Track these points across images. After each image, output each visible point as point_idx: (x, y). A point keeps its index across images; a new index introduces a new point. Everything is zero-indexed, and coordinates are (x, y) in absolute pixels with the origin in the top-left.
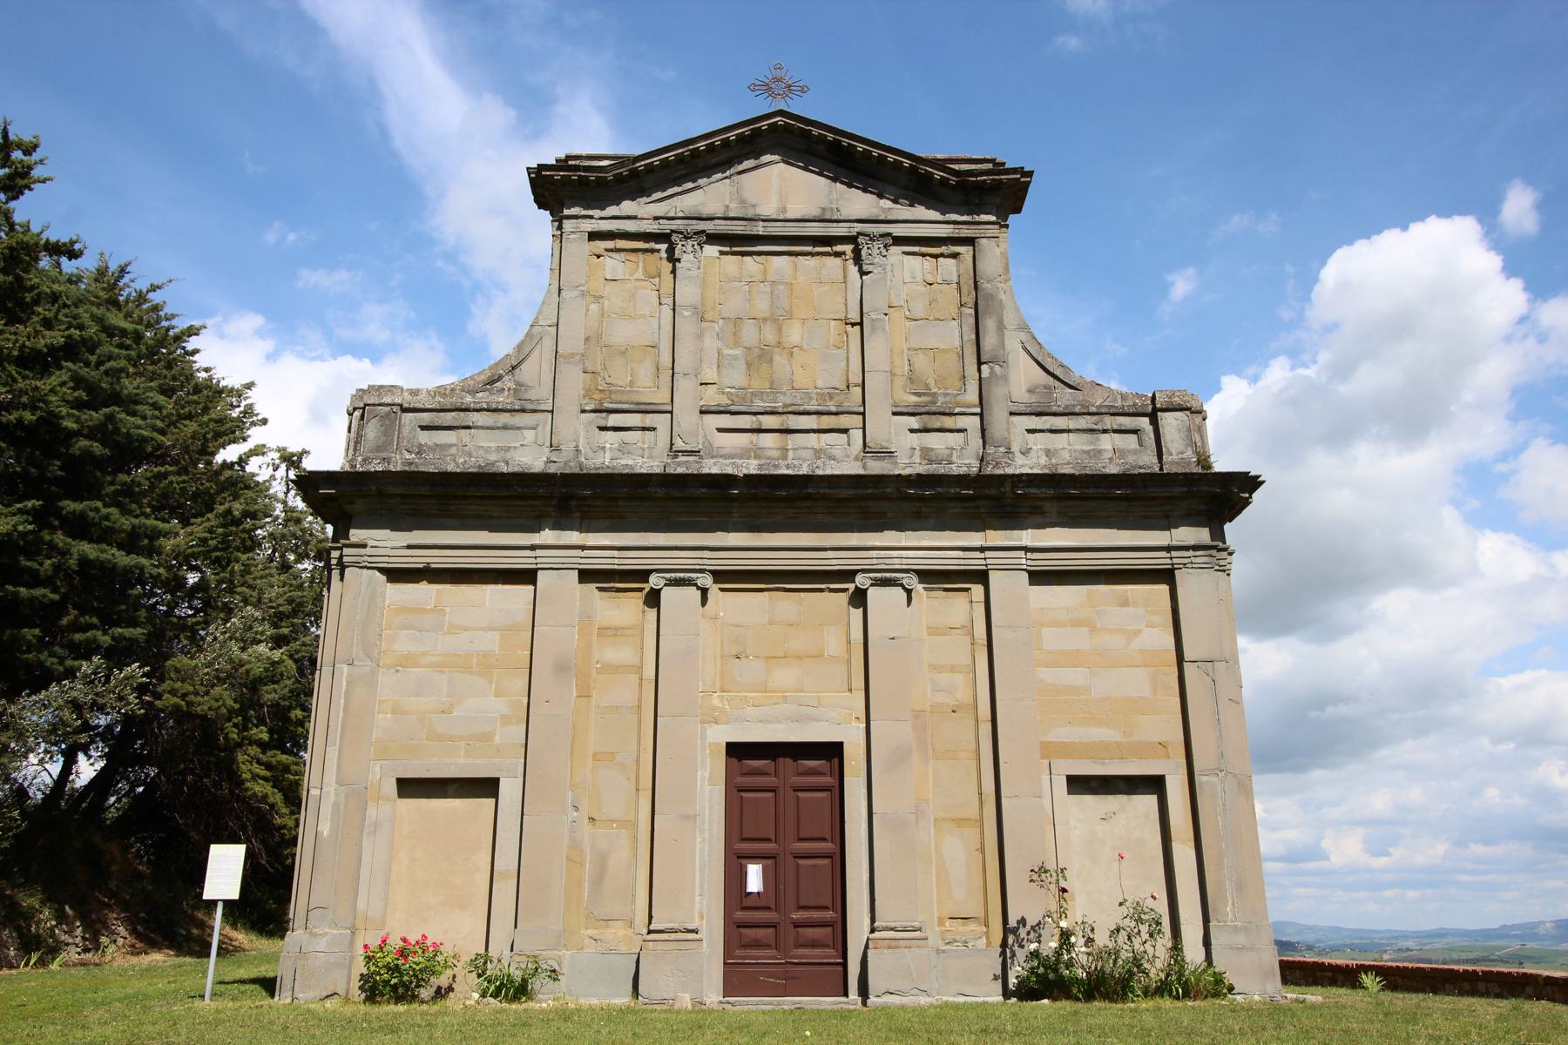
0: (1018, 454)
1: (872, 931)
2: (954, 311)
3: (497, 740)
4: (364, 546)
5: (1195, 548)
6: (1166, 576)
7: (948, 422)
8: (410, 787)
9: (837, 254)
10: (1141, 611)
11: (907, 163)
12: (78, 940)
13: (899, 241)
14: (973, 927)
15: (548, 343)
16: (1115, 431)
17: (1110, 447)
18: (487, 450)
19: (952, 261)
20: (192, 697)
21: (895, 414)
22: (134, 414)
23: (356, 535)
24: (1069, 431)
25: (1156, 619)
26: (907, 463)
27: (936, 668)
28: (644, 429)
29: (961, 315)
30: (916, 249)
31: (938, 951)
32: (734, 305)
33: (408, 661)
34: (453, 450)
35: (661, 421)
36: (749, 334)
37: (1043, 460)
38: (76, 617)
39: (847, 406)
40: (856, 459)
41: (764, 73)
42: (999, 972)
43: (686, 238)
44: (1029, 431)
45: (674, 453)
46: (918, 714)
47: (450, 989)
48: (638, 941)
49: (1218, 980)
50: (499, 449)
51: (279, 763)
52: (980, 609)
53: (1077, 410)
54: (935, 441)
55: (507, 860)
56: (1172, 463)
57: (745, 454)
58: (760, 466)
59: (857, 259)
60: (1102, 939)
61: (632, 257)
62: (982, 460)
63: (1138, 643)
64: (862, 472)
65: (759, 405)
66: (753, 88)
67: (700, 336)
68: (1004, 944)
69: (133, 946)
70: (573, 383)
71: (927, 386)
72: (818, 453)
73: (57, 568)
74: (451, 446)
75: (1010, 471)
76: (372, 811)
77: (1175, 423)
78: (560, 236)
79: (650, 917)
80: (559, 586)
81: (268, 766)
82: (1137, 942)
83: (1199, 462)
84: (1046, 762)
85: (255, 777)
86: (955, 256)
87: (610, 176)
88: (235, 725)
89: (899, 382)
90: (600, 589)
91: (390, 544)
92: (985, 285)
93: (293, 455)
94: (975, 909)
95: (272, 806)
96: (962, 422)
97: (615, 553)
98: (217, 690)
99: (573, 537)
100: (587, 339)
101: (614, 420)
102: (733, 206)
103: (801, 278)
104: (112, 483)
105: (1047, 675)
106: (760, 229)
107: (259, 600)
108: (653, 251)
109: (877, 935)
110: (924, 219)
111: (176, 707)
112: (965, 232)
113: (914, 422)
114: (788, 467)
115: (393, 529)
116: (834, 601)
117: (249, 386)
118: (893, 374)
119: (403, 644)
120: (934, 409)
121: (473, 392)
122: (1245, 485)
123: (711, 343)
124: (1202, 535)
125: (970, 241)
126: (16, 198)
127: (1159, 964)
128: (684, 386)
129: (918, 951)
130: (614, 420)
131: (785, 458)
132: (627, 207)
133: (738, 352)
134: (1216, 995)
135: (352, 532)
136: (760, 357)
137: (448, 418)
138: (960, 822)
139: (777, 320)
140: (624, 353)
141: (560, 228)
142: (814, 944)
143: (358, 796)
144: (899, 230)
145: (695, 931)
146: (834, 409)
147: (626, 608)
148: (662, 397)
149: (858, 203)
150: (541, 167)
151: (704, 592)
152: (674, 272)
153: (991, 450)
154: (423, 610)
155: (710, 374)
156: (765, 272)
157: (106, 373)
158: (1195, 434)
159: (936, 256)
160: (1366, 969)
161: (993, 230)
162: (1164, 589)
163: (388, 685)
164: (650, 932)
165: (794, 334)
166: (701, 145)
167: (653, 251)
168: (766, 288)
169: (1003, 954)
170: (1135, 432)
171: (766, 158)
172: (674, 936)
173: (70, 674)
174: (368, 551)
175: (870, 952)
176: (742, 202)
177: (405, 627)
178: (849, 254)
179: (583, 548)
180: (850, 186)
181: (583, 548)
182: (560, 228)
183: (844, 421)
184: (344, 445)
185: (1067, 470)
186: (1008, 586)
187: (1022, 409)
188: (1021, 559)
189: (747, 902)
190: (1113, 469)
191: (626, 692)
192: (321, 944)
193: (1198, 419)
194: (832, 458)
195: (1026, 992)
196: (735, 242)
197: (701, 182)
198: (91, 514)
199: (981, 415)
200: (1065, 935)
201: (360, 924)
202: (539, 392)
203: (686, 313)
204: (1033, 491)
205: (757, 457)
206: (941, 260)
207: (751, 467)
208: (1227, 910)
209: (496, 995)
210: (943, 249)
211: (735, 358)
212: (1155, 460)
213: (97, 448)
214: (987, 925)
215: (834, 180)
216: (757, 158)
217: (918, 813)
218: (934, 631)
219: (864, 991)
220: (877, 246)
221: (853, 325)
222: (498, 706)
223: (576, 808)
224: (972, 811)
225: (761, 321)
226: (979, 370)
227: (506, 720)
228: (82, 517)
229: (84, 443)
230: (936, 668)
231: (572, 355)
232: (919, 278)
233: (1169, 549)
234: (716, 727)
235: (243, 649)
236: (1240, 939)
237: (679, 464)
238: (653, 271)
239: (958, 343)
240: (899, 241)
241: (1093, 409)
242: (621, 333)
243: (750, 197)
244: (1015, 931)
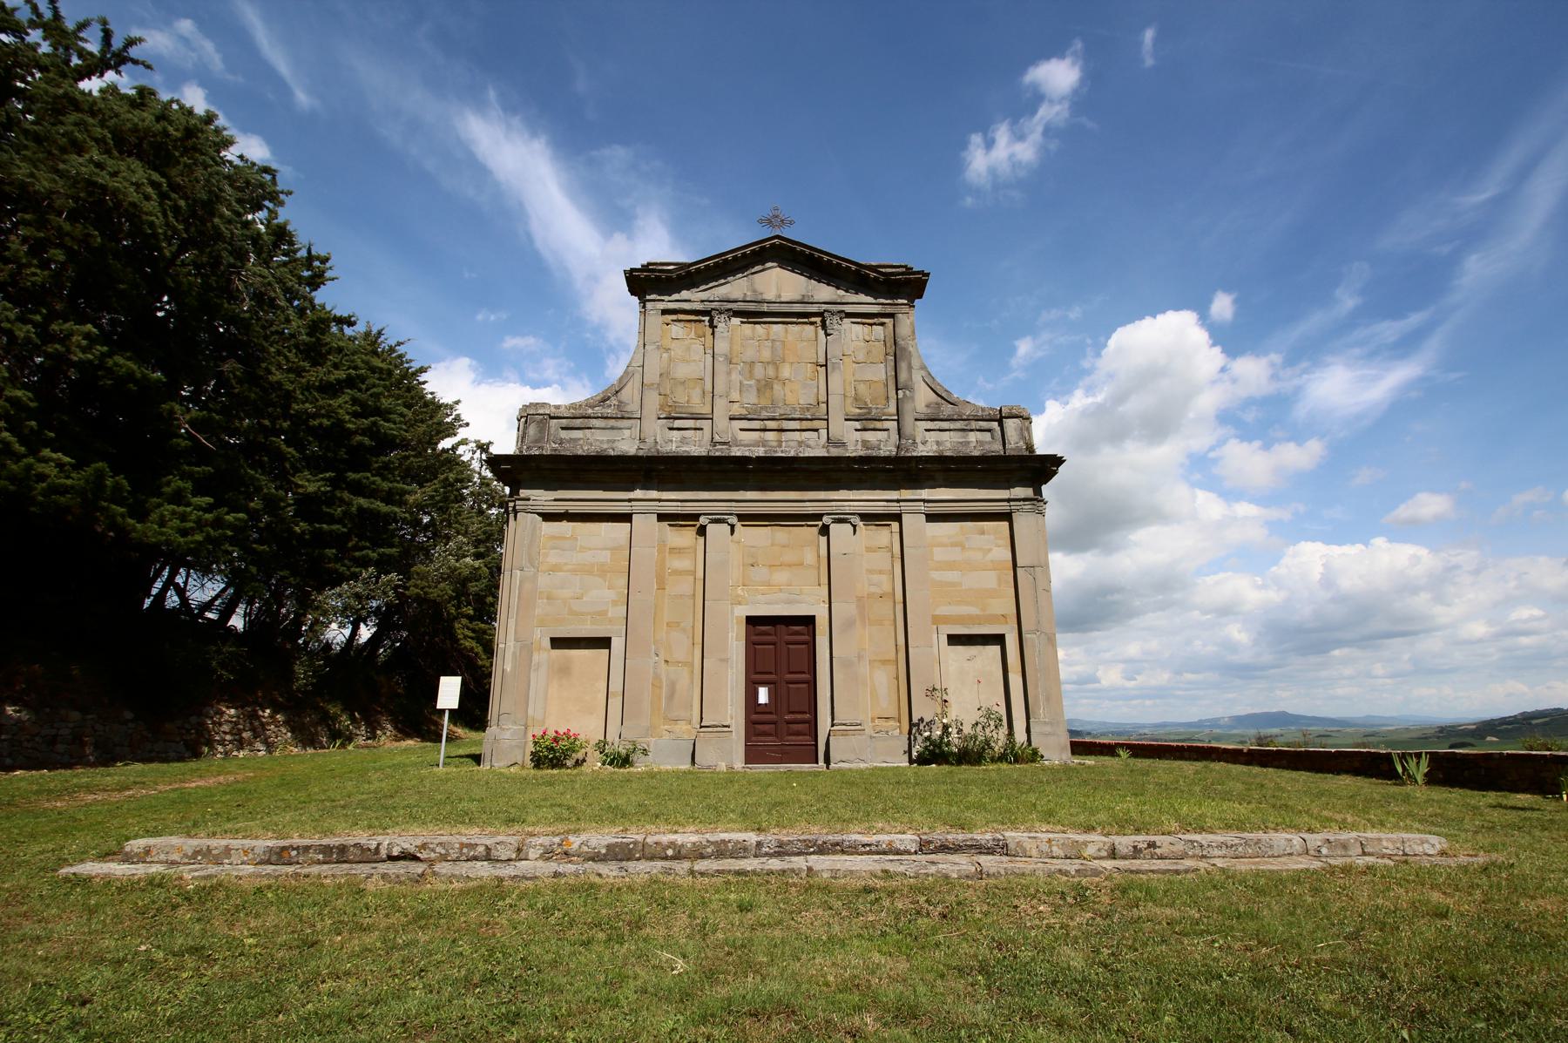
0: (920, 444)
1: (833, 726)
2: (882, 358)
3: (610, 615)
4: (529, 500)
5: (1025, 500)
6: (1007, 517)
7: (878, 425)
9: (812, 323)
10: (992, 537)
11: (853, 268)
12: (363, 733)
13: (849, 315)
14: (891, 723)
15: (638, 377)
16: (978, 430)
17: (974, 440)
18: (602, 442)
19: (881, 328)
20: (427, 589)
21: (846, 420)
22: (388, 421)
23: (523, 493)
24: (950, 430)
25: (1001, 542)
26: (853, 450)
27: (870, 572)
28: (696, 429)
29: (886, 360)
30: (859, 320)
31: (871, 737)
32: (750, 354)
33: (555, 568)
34: (581, 442)
35: (706, 424)
36: (759, 371)
37: (935, 447)
38: (357, 542)
39: (818, 415)
40: (823, 447)
41: (768, 213)
42: (907, 749)
43: (721, 313)
44: (926, 430)
45: (714, 443)
46: (860, 599)
47: (584, 760)
48: (694, 732)
49: (1035, 752)
50: (608, 441)
51: (480, 629)
52: (897, 537)
53: (955, 417)
54: (870, 436)
55: (616, 685)
56: (1012, 449)
57: (757, 444)
58: (766, 452)
59: (824, 326)
60: (967, 730)
61: (688, 325)
62: (898, 448)
63: (990, 556)
64: (826, 455)
65: (765, 414)
66: (760, 221)
67: (729, 373)
68: (910, 733)
69: (395, 736)
70: (653, 401)
71: (866, 403)
72: (800, 443)
73: (345, 513)
74: (580, 439)
75: (915, 454)
76: (536, 657)
77: (1013, 425)
78: (644, 312)
79: (702, 718)
80: (645, 524)
81: (473, 631)
82: (988, 730)
83: (1027, 449)
84: (935, 627)
85: (466, 637)
86: (882, 324)
87: (674, 275)
88: (453, 606)
89: (849, 401)
90: (670, 525)
91: (543, 498)
92: (901, 342)
93: (484, 445)
94: (894, 713)
95: (477, 654)
96: (887, 425)
97: (679, 504)
98: (442, 585)
99: (654, 494)
100: (661, 375)
101: (678, 423)
102: (749, 293)
103: (790, 338)
104: (376, 462)
105: (936, 575)
106: (765, 308)
107: (466, 532)
108: (700, 321)
109: (835, 728)
110: (863, 302)
111: (418, 594)
112: (889, 310)
113: (858, 425)
114: (782, 452)
115: (546, 490)
116: (809, 532)
117: (457, 402)
118: (845, 396)
119: (553, 558)
120: (870, 417)
121: (592, 407)
122: (1057, 461)
123: (735, 377)
124: (1028, 492)
125: (891, 316)
126: (316, 290)
127: (1000, 743)
128: (720, 404)
129: (860, 737)
130: (678, 423)
131: (781, 446)
132: (685, 294)
133: (752, 382)
134: (1033, 761)
135: (521, 491)
136: (765, 386)
137: (578, 422)
138: (885, 662)
139: (775, 363)
140: (683, 383)
141: (644, 307)
142: (798, 734)
143: (527, 649)
144: (848, 309)
145: (728, 727)
146: (809, 417)
147: (685, 537)
148: (706, 410)
149: (825, 292)
150: (633, 270)
151: (733, 527)
152: (713, 334)
153: (903, 442)
154: (566, 538)
155: (735, 396)
156: (768, 334)
157: (371, 395)
158: (1026, 432)
159: (871, 325)
160: (1121, 745)
161: (906, 309)
162: (1006, 524)
163: (543, 581)
164: (701, 727)
166: (729, 256)
167: (700, 321)
168: (769, 344)
169: (909, 739)
170: (989, 430)
171: (769, 265)
172: (715, 729)
173: (355, 577)
174: (531, 502)
175: (831, 738)
176: (754, 291)
177: (554, 548)
178: (819, 323)
179: (660, 500)
180: (819, 281)
181: (660, 500)
182: (644, 307)
183: (816, 424)
184: (515, 439)
185: (948, 454)
186: (914, 523)
187: (923, 417)
188: (922, 507)
189: (759, 709)
190: (976, 453)
191: (685, 586)
192: (507, 735)
193: (1027, 423)
194: (808, 446)
195: (923, 760)
197: (730, 279)
198: (365, 481)
199: (898, 420)
200: (946, 727)
201: (530, 723)
202: (633, 407)
203: (721, 359)
204: (929, 466)
205: (763, 446)
206: (874, 327)
207: (760, 452)
208: (1041, 712)
209: (611, 763)
210: (875, 320)
211: (750, 386)
212: (1001, 448)
213: (367, 441)
214: (900, 722)
215: (810, 278)
216: (763, 264)
217: (860, 657)
218: (869, 549)
219: (827, 760)
220: (836, 318)
221: (821, 366)
222: (610, 595)
223: (657, 655)
224: (892, 656)
225: (766, 364)
226: (897, 394)
227: (615, 603)
228: (359, 482)
229: (359, 438)
230: (870, 572)
231: (652, 384)
232: (861, 337)
233: (1009, 500)
234: (740, 607)
235: (457, 561)
236: (1048, 729)
237: (717, 450)
238: (701, 333)
239: (884, 377)
240: (849, 315)
241: (965, 417)
242: (681, 371)
243: (760, 288)
244: (918, 725)
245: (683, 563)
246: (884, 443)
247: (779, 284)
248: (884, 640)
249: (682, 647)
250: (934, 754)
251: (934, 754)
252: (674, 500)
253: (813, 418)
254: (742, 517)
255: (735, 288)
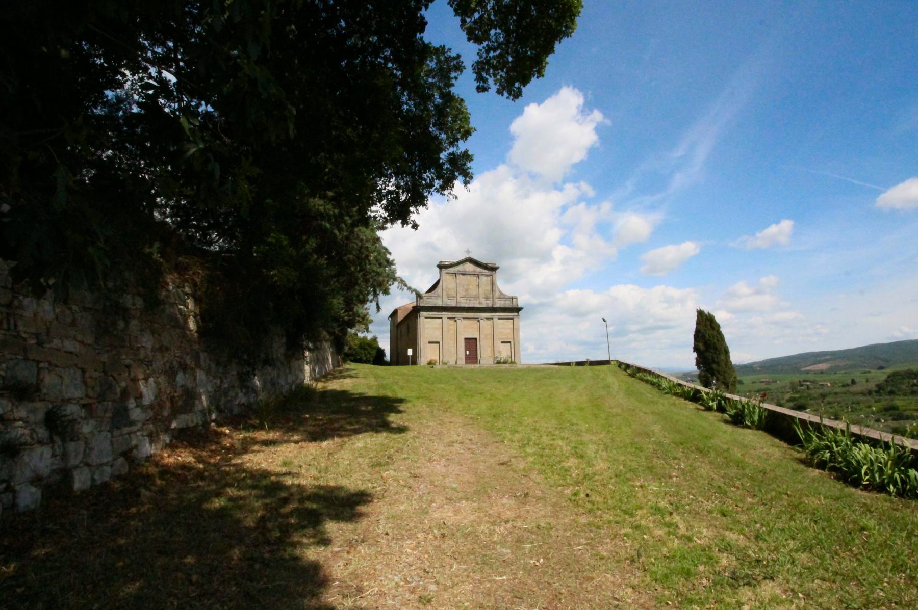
6: (512, 319)
8: (430, 343)
26: (484, 306)
72: (474, 303)
80: (445, 320)
110: (486, 272)
116: (476, 321)
124: (516, 314)
128: (458, 294)
136: (467, 290)
147: (452, 322)
149: (478, 270)
158: (517, 302)
165: (471, 287)
186: (495, 320)
196: (463, 274)
208: (516, 355)
245: (452, 327)
246: (489, 303)
247: (469, 267)
248: (490, 342)
249: (452, 343)
250: (499, 363)
251: (499, 363)
252: (450, 314)
253: (477, 297)
254: (463, 318)
255: (460, 268)
